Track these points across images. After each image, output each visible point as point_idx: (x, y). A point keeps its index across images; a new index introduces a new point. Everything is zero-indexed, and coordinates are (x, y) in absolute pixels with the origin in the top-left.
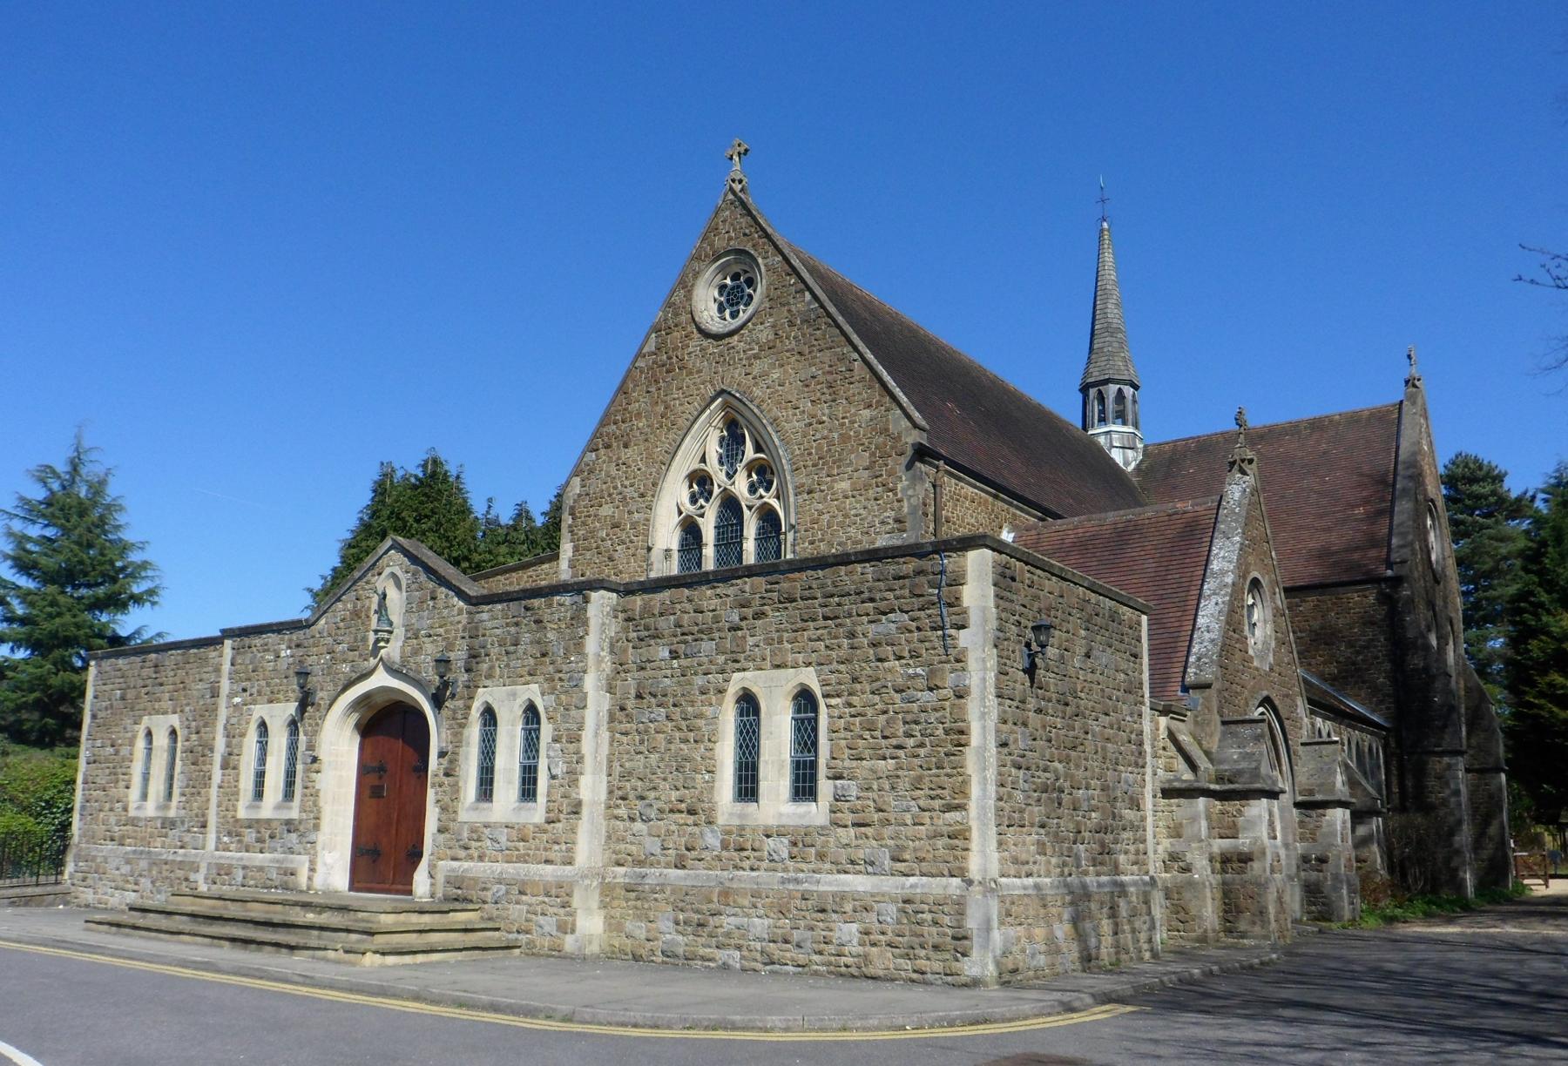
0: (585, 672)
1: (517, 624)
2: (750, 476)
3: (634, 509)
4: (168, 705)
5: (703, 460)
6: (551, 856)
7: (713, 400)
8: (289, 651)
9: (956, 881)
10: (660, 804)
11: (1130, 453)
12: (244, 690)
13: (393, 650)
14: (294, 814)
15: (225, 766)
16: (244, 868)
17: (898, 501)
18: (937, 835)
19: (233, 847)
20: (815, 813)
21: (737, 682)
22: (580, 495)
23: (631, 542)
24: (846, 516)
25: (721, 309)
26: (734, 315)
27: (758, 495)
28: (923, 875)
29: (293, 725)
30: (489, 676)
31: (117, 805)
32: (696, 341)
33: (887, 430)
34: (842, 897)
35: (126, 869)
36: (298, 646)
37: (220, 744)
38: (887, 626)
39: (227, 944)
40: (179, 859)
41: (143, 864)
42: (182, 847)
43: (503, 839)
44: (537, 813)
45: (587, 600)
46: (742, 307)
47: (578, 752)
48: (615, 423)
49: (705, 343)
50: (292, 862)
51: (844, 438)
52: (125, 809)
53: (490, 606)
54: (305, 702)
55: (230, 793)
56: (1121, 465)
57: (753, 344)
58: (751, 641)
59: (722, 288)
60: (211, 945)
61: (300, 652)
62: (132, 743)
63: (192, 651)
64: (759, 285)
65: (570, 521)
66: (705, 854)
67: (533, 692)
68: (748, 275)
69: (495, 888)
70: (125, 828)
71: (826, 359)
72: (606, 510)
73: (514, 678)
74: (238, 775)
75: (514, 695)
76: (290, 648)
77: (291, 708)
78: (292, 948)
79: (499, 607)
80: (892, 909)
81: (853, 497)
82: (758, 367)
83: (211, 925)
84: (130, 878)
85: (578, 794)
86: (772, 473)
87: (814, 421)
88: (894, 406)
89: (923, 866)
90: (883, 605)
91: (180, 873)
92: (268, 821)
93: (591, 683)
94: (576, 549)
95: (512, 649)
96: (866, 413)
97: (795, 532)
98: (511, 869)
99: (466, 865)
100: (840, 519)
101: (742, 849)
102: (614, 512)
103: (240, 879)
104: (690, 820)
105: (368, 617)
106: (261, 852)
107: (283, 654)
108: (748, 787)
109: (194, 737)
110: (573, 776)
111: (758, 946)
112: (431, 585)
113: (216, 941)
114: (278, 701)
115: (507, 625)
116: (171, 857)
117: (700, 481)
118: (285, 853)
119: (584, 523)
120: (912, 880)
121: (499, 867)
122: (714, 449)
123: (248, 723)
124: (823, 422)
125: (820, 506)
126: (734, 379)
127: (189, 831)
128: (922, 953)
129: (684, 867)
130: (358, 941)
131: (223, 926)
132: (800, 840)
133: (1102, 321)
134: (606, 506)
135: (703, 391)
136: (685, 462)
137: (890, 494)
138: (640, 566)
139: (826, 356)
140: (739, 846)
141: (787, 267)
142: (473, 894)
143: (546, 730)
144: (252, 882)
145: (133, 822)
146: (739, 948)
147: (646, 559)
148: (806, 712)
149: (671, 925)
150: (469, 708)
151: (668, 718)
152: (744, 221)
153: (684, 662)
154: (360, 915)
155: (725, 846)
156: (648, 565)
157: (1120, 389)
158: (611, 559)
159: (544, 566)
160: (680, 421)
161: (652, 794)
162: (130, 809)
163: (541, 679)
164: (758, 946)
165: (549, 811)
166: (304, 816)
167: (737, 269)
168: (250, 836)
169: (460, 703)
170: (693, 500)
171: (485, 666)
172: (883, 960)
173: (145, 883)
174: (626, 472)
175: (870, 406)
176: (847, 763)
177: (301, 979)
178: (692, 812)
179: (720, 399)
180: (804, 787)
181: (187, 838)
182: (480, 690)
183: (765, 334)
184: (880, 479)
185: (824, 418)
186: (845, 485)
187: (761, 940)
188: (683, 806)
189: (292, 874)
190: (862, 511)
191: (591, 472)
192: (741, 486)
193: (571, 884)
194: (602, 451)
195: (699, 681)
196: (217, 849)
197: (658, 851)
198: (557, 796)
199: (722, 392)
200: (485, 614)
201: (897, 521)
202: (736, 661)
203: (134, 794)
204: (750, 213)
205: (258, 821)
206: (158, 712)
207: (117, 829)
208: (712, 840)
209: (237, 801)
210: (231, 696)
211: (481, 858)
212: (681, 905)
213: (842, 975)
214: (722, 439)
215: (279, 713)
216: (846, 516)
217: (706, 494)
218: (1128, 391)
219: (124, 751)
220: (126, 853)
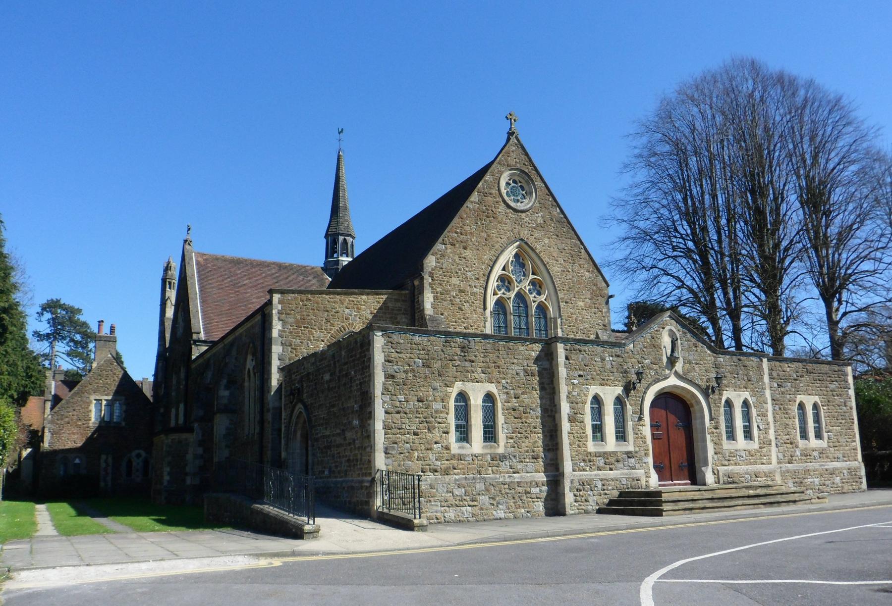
0: (765, 389)
1: (736, 366)
2: (529, 285)
3: (473, 285)
6: (764, 461)
7: (517, 241)
8: (611, 358)
9: (856, 462)
10: (781, 441)
12: (580, 376)
13: (679, 367)
14: (631, 448)
15: (571, 420)
16: (601, 480)
17: (603, 317)
18: (852, 449)
19: (588, 468)
21: (799, 398)
22: (436, 267)
23: (473, 303)
24: (583, 317)
27: (533, 295)
28: (850, 461)
29: (619, 401)
32: (502, 208)
33: (597, 285)
34: (835, 469)
35: (459, 492)
36: (618, 356)
38: (832, 386)
39: (762, 506)
40: (517, 480)
41: (480, 486)
42: (514, 473)
43: (744, 456)
44: (754, 445)
45: (762, 361)
46: (512, 198)
47: (767, 420)
48: (456, 233)
49: (508, 211)
50: (637, 474)
52: (447, 448)
53: (723, 356)
54: (629, 388)
55: (579, 439)
57: (533, 222)
58: (801, 385)
60: (754, 509)
61: (620, 360)
63: (501, 343)
64: (534, 194)
65: (430, 280)
66: (797, 458)
67: (746, 395)
68: (521, 184)
69: (746, 476)
70: (448, 462)
71: (569, 243)
72: (455, 281)
73: (736, 388)
74: (585, 426)
75: (740, 396)
76: (612, 356)
77: (619, 390)
78: (795, 502)
79: (728, 357)
80: (845, 472)
82: (537, 234)
83: (723, 502)
84: (465, 498)
87: (565, 271)
88: (599, 275)
90: (833, 379)
91: (520, 489)
92: (615, 453)
93: (768, 393)
94: (435, 298)
95: (736, 376)
97: (561, 319)
98: (750, 468)
99: (731, 468)
102: (460, 283)
103: (600, 486)
104: (791, 446)
105: (661, 348)
106: (611, 469)
107: (607, 359)
108: (804, 436)
109: (515, 400)
111: (817, 487)
112: (694, 340)
113: (756, 506)
114: (607, 385)
115: (732, 365)
116: (507, 480)
118: (628, 469)
119: (441, 284)
120: (848, 463)
121: (744, 468)
123: (586, 396)
125: (571, 311)
126: (525, 234)
127: (522, 462)
128: (854, 484)
129: (792, 463)
130: (799, 496)
131: (730, 501)
132: (822, 452)
133: (343, 203)
134: (455, 279)
138: (479, 317)
139: (569, 242)
140: (806, 454)
141: (547, 191)
142: (736, 480)
143: (754, 412)
144: (610, 488)
145: (460, 458)
146: (812, 489)
147: (483, 315)
148: (488, 403)
149: (792, 484)
150: (721, 399)
151: (780, 409)
152: (523, 157)
153: (783, 389)
154: (775, 488)
155: (802, 455)
157: (345, 239)
158: (460, 309)
159: (364, 297)
160: (497, 246)
161: (779, 437)
162: (452, 449)
163: (749, 390)
164: (817, 487)
165: (760, 443)
166: (637, 449)
167: (517, 178)
169: (717, 397)
172: (847, 487)
173: (484, 499)
174: (466, 263)
175: (589, 272)
176: (830, 428)
177: (861, 506)
178: (791, 443)
179: (518, 243)
180: (819, 436)
181: (520, 466)
182: (724, 392)
184: (596, 305)
185: (570, 270)
186: (581, 304)
187: (817, 485)
188: (789, 441)
189: (638, 480)
190: (589, 317)
191: (443, 256)
193: (775, 471)
194: (449, 246)
195: (788, 397)
196: (573, 471)
197: (782, 458)
198: (762, 438)
199: (522, 240)
201: (604, 325)
202: (798, 391)
203: (453, 436)
204: (527, 154)
205: (605, 453)
207: (438, 463)
208: (798, 453)
209: (587, 441)
210: (569, 378)
211: (736, 464)
212: (794, 477)
213: (838, 493)
214: (512, 261)
215: (610, 394)
216: (583, 317)
217: (505, 287)
218: (349, 239)
219: (437, 406)
220: (456, 480)
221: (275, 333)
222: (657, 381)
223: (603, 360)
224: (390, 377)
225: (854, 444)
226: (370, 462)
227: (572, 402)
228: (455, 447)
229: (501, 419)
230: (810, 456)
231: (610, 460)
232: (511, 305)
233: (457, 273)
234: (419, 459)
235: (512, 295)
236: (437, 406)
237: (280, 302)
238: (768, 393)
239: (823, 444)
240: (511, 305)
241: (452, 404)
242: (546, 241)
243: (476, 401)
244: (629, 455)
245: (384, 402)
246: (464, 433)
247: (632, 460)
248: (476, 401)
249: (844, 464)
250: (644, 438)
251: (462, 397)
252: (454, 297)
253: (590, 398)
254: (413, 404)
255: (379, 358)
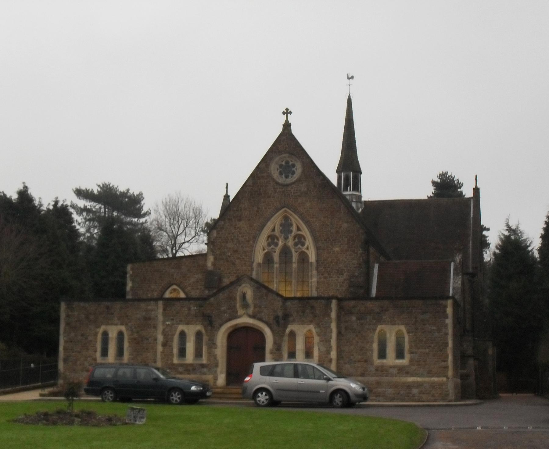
2: (294, 239)
4: (116, 320)
5: (274, 230)
11: (359, 205)
12: (173, 320)
14: (204, 361)
15: (164, 345)
20: (404, 362)
22: (216, 237)
25: (281, 173)
26: (287, 177)
30: (293, 321)
31: (89, 359)
37: (160, 338)
45: (331, 302)
51: (337, 232)
52: (95, 359)
55: (168, 355)
56: (356, 210)
59: (281, 166)
62: (96, 334)
72: (230, 245)
73: (303, 323)
81: (341, 253)
82: (300, 200)
85: (330, 356)
86: (305, 239)
89: (438, 375)
92: (191, 365)
94: (215, 259)
96: (345, 225)
100: (336, 261)
101: (383, 371)
110: (328, 352)
117: (272, 239)
122: (278, 228)
123: (176, 331)
124: (329, 225)
135: (276, 205)
136: (266, 232)
137: (356, 254)
140: (382, 370)
147: (251, 266)
155: (377, 370)
156: (252, 268)
166: (209, 363)
168: (180, 369)
170: (269, 245)
171: (291, 319)
183: (303, 188)
185: (329, 224)
186: (337, 249)
192: (290, 243)
200: (289, 303)
203: (98, 354)
206: (112, 324)
208: (373, 369)
210: (164, 322)
219: (90, 338)
221: (128, 288)
222: (230, 320)
223: (189, 309)
224: (68, 324)
225: (445, 363)
226: (56, 366)
227: (164, 333)
228: (99, 360)
229: (126, 345)
230: (386, 371)
231: (189, 369)
232: (276, 257)
233: (232, 239)
234: (80, 365)
235: (278, 250)
236: (90, 338)
237: (132, 269)
238: (333, 326)
239: (404, 362)
240: (276, 257)
241: (99, 337)
242: (308, 204)
243: (113, 334)
244: (203, 366)
245: (64, 337)
246: (105, 353)
247: (205, 370)
248: (113, 334)
249: (427, 379)
250: (215, 357)
251: (105, 335)
252: (229, 256)
253: (178, 332)
254: (79, 337)
255: (63, 315)
